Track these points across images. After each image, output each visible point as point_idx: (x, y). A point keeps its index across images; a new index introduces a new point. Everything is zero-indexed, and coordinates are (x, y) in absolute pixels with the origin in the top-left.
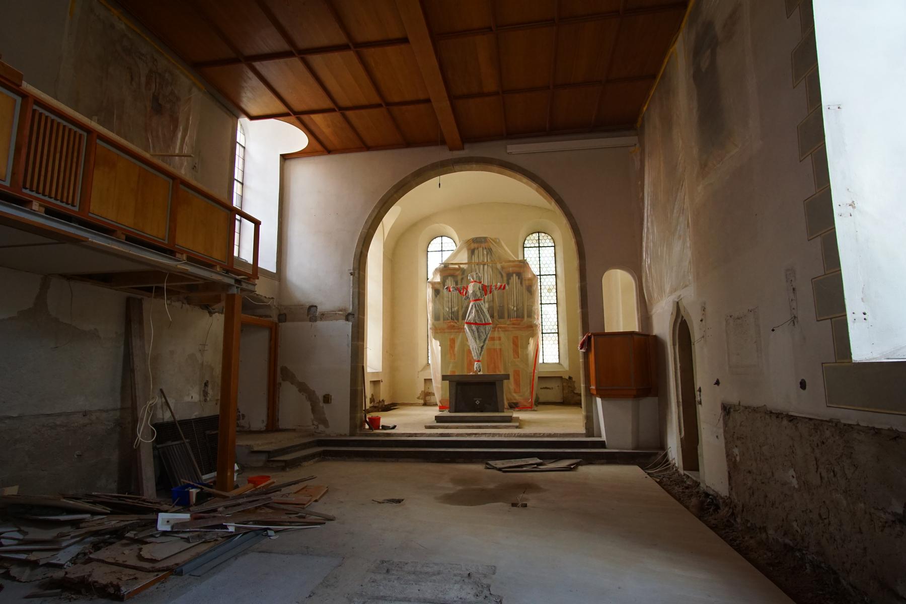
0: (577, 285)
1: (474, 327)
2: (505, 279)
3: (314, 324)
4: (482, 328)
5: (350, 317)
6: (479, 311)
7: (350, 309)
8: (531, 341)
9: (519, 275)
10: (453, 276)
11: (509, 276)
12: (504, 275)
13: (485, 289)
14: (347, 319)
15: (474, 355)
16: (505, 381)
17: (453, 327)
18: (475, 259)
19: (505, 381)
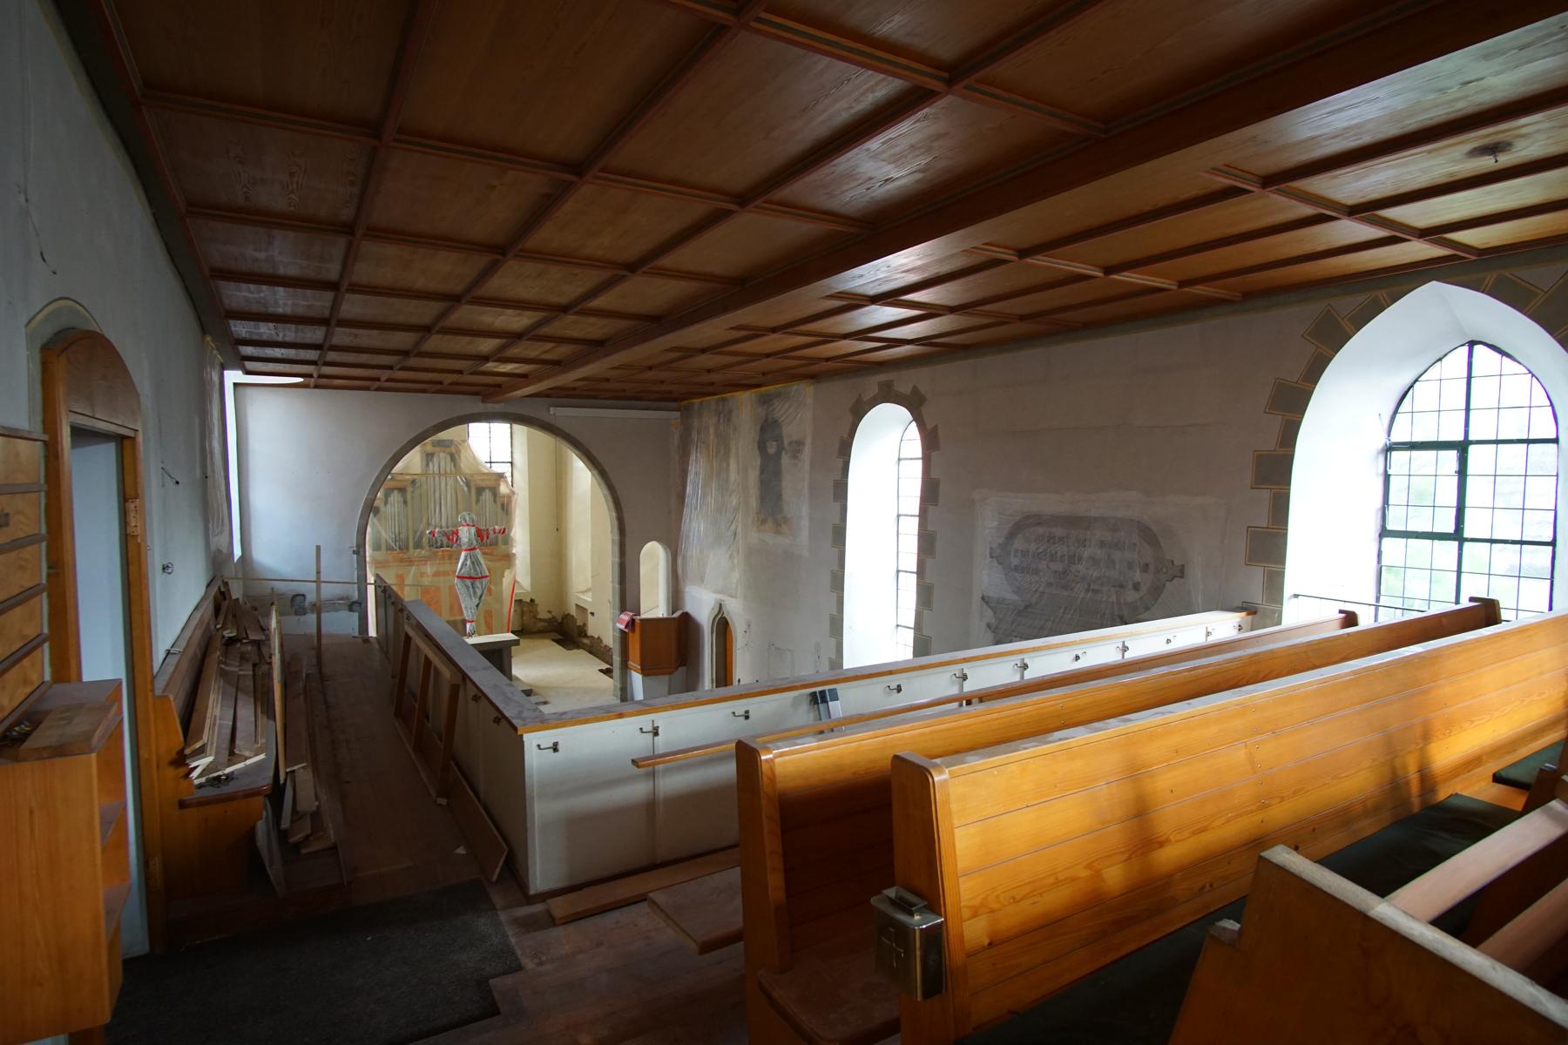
0: (617, 560)
1: (468, 582)
2: (474, 497)
3: (303, 618)
4: (477, 583)
5: (355, 607)
6: (475, 563)
7: (356, 596)
8: (507, 573)
9: (494, 491)
10: (402, 490)
11: (480, 490)
12: (473, 491)
13: (479, 533)
14: (351, 609)
15: (467, 615)
16: (514, 648)
17: (402, 560)
18: (434, 467)
19: (514, 648)
